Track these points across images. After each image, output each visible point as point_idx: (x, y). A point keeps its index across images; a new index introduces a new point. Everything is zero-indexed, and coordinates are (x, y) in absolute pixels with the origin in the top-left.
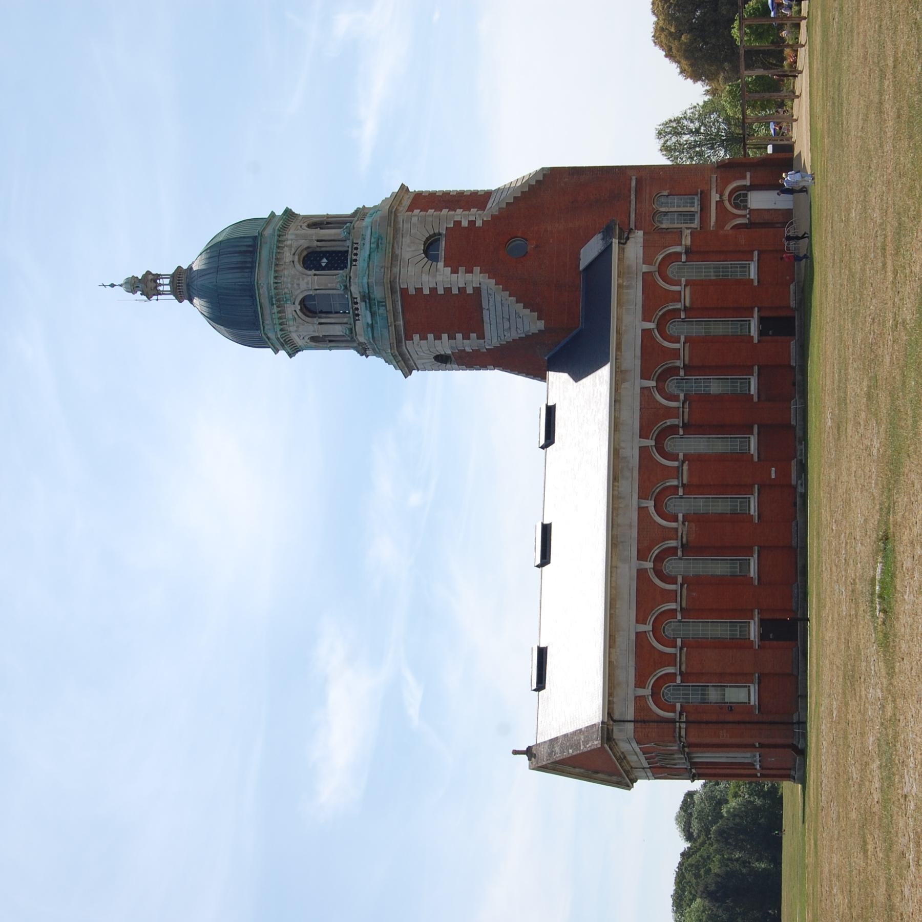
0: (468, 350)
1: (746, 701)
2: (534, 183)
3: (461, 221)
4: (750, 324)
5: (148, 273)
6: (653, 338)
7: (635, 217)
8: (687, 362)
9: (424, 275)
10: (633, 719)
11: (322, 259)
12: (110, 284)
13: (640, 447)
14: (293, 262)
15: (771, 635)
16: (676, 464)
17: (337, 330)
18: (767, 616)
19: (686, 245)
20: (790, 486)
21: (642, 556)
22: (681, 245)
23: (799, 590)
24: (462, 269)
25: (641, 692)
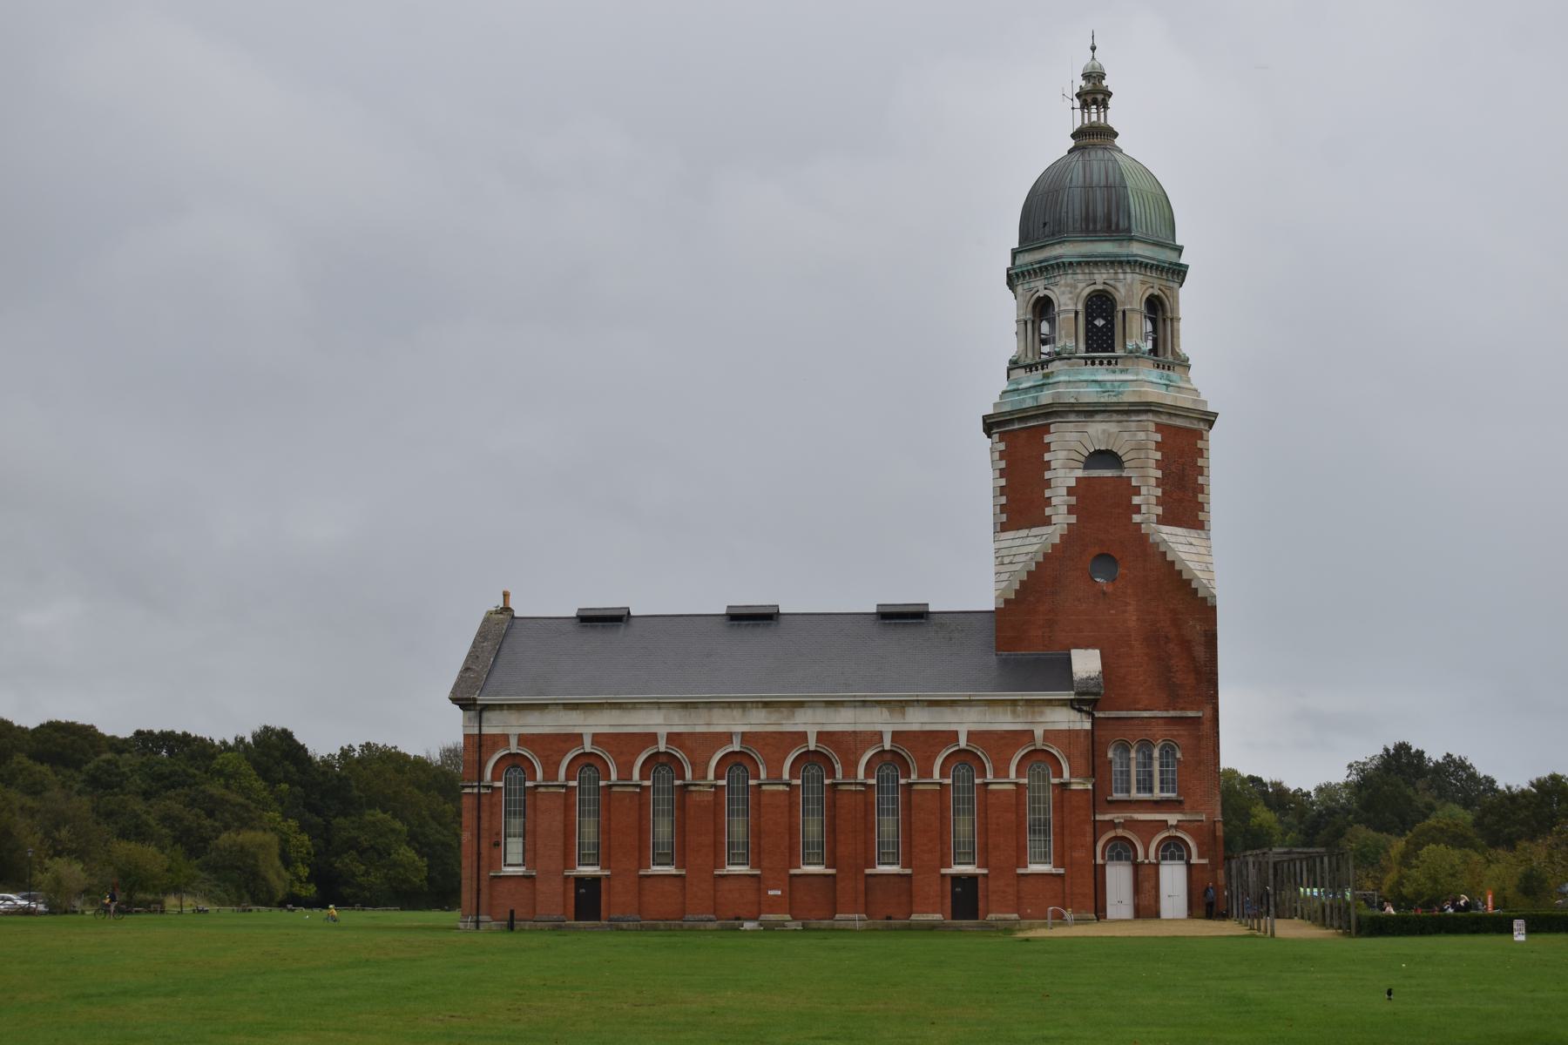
1: (508, 862)
2: (1193, 586)
3: (1139, 495)
4: (969, 864)
5: (1110, 94)
6: (946, 745)
7: (1146, 718)
8: (916, 787)
9: (1065, 453)
10: (483, 733)
11: (1104, 318)
12: (1096, 44)
13: (806, 733)
14: (1095, 283)
15: (960, 889)
16: (786, 776)
19: (1070, 783)
20: (760, 914)
21: (672, 738)
22: (1071, 776)
23: (631, 923)
25: (513, 742)
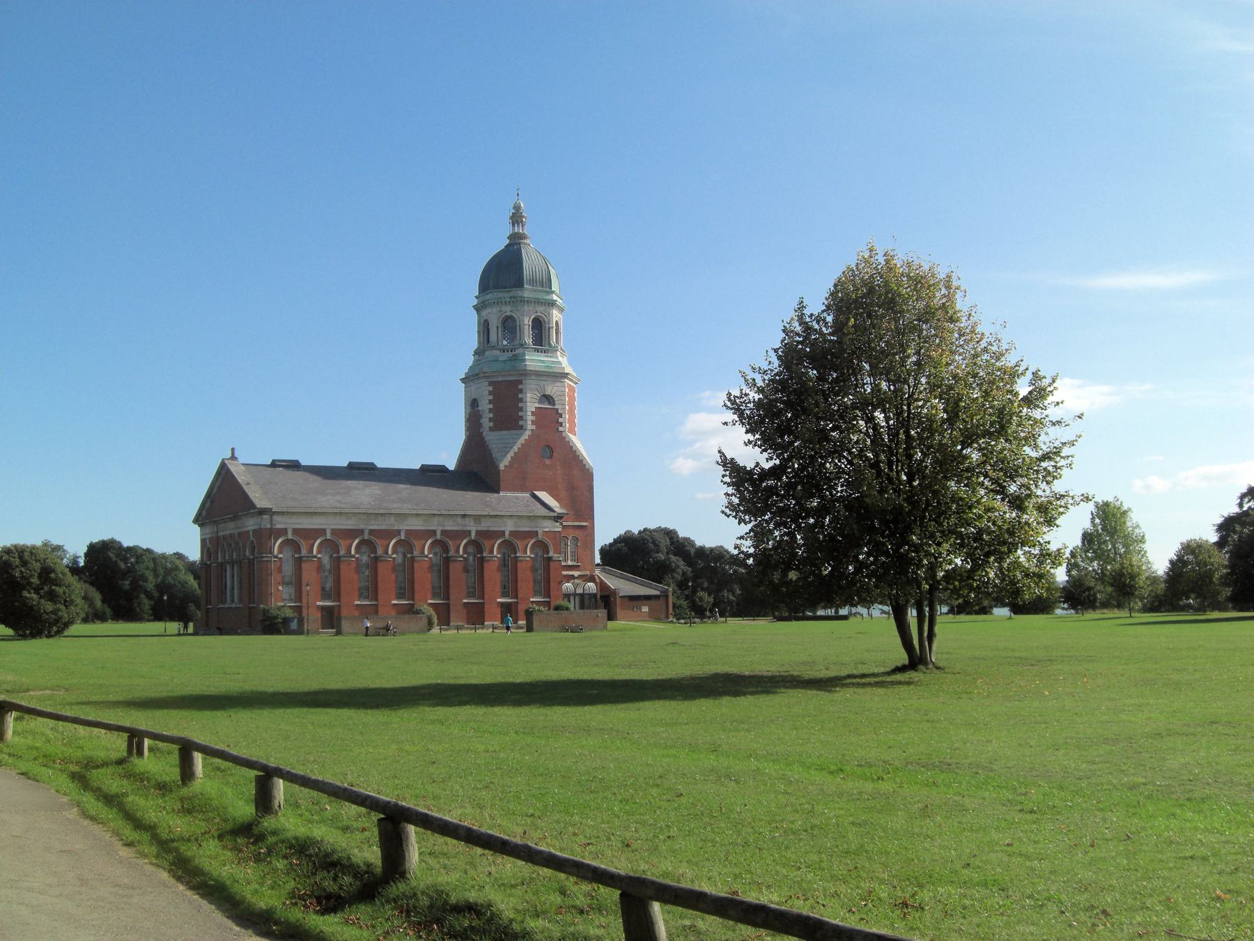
0: (482, 421)
17: (493, 337)
18: (336, 610)
24: (534, 418)
25: (290, 532)
